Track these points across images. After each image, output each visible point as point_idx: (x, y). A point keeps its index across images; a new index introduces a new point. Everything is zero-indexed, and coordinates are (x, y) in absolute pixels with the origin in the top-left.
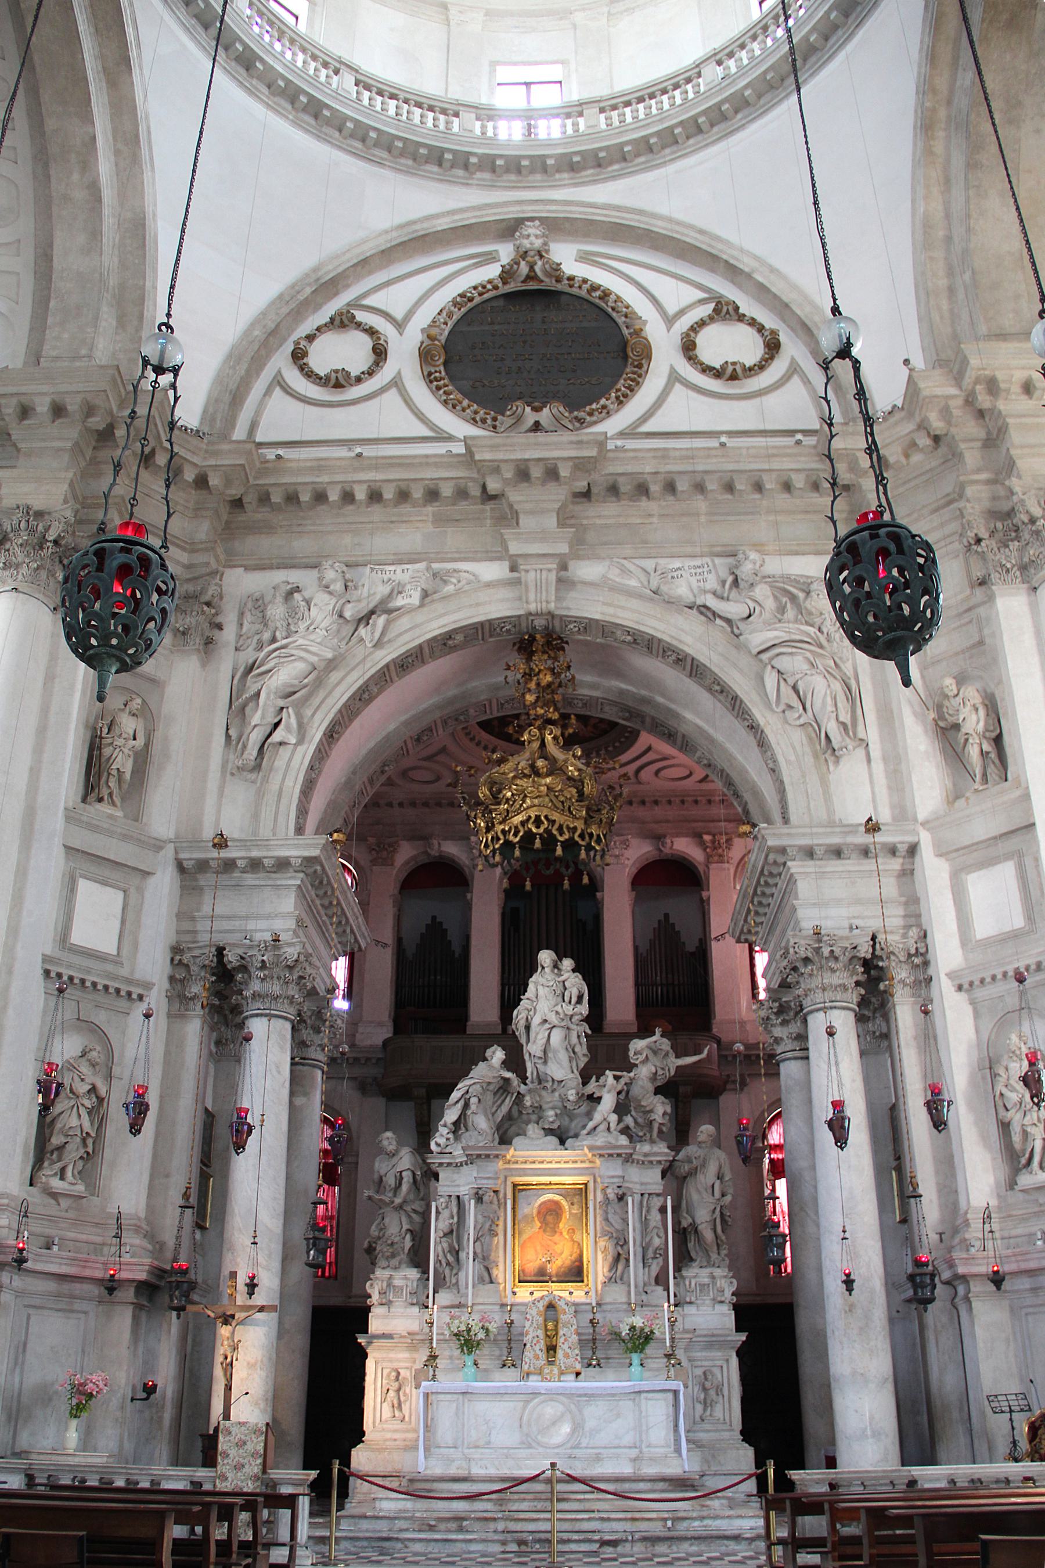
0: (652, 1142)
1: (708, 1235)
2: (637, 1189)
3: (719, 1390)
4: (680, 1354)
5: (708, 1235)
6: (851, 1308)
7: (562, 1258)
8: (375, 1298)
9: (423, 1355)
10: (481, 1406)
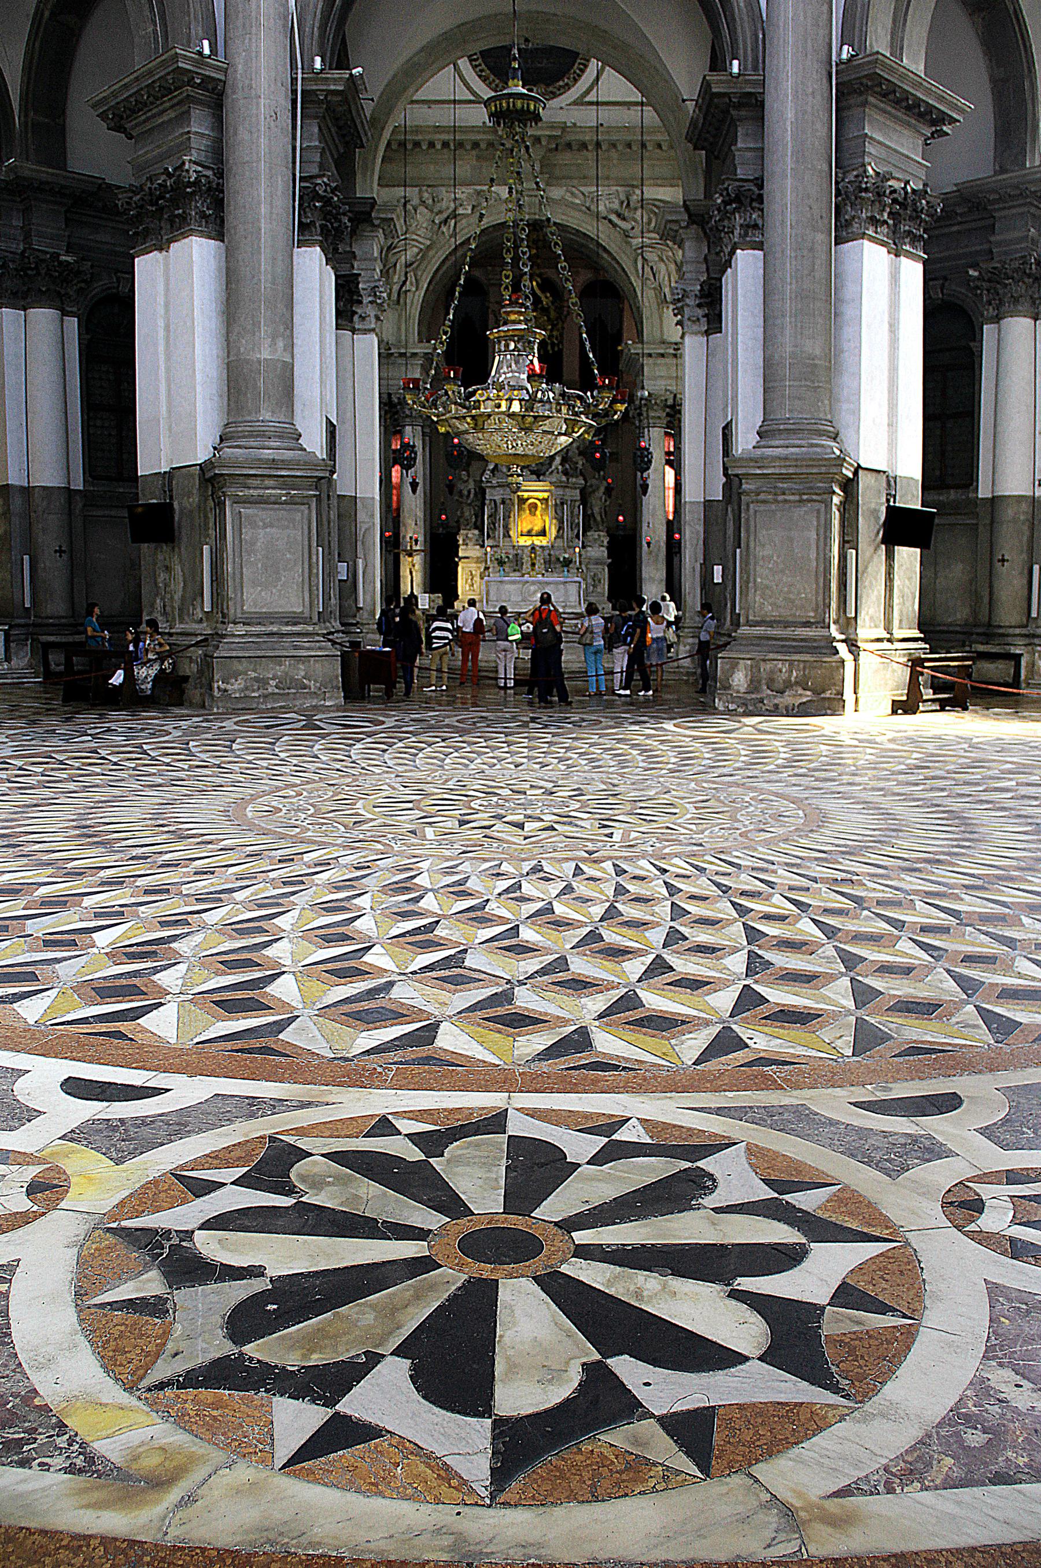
0: (577, 477)
1: (599, 518)
2: (569, 498)
3: (600, 581)
4: (584, 567)
5: (599, 518)
6: (651, 553)
7: (537, 528)
8: (461, 542)
9: (483, 566)
10: (507, 586)
